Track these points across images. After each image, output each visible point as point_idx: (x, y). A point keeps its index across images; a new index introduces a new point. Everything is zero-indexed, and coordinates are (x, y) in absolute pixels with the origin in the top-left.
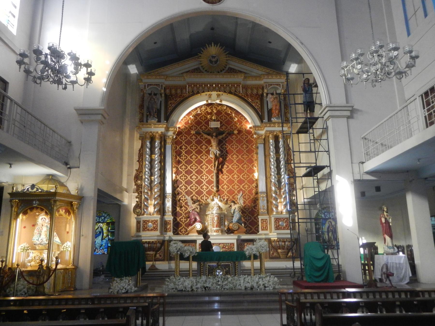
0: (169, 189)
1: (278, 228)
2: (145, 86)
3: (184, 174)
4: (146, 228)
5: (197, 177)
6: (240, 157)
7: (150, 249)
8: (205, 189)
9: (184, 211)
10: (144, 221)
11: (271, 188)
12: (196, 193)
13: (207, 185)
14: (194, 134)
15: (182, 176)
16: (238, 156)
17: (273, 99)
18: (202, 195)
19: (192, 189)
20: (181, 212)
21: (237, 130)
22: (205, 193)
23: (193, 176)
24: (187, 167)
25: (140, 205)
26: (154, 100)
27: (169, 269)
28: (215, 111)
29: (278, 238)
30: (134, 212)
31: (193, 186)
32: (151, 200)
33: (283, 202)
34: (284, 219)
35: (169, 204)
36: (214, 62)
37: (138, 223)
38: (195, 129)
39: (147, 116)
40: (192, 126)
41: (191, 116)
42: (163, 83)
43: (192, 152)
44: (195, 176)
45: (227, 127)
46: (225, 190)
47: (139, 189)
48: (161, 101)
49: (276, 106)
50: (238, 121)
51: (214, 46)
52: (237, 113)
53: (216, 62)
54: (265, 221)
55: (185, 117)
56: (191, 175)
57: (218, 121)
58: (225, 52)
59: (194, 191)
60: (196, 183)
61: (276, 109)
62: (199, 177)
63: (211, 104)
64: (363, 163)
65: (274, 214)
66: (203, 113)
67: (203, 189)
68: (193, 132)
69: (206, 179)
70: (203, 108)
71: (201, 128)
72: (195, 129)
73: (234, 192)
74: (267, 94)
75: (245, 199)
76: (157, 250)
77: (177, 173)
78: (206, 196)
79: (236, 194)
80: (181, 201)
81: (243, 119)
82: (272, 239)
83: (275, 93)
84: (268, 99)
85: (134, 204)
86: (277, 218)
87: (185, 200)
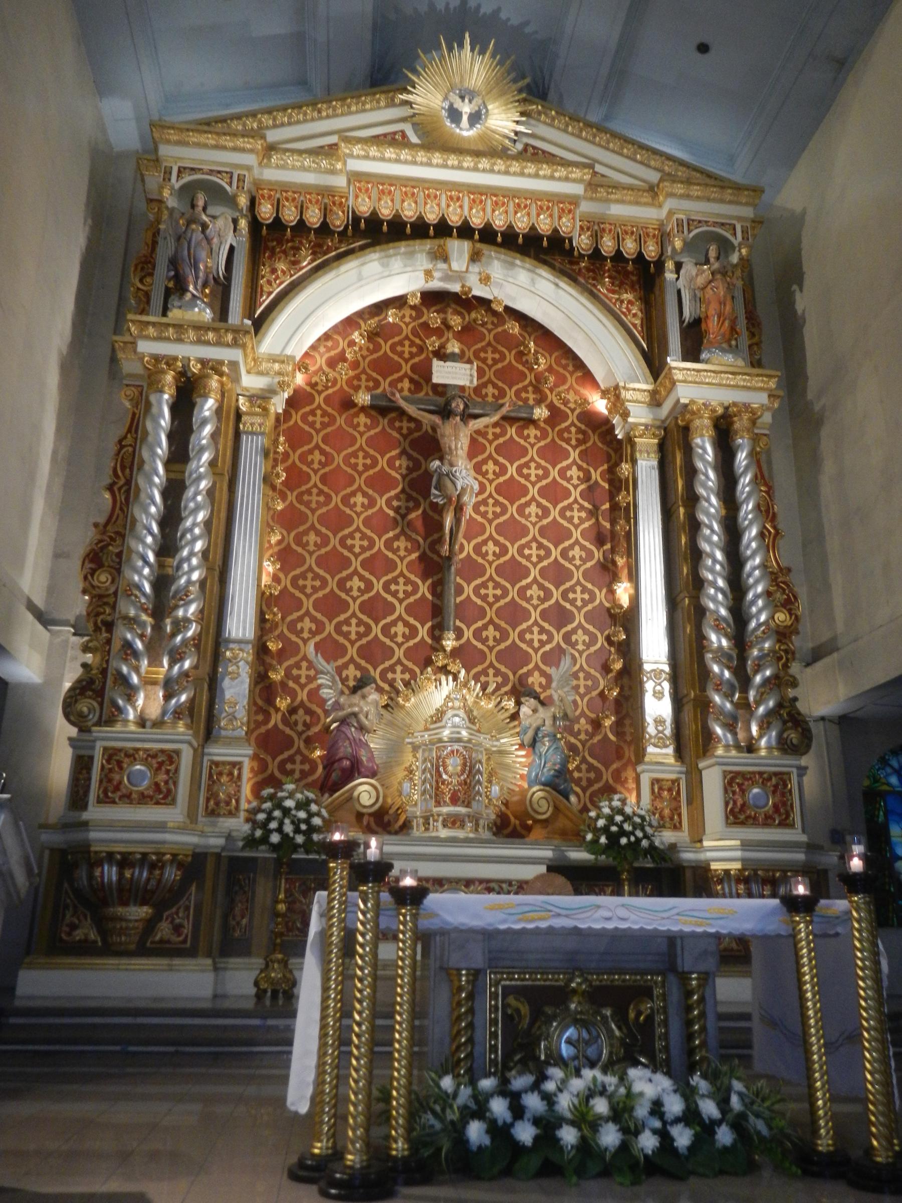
0: (241, 623)
1: (738, 815)
2: (168, 172)
3: (310, 569)
4: (117, 788)
5: (369, 586)
6: (555, 513)
7: (128, 893)
8: (400, 639)
9: (300, 728)
10: (111, 754)
12: (364, 652)
13: (412, 620)
14: (363, 409)
15: (303, 576)
16: (546, 512)
17: (707, 275)
18: (387, 664)
19: (346, 635)
20: (288, 731)
21: (548, 407)
22: (399, 653)
23: (350, 577)
24: (326, 541)
25: (97, 685)
26: (204, 226)
27: (215, 996)
29: (743, 860)
30: (67, 715)
31: (347, 622)
32: (155, 661)
33: (758, 703)
34: (764, 778)
35: (237, 689)
36: (465, 118)
37: (82, 764)
39: (168, 293)
41: (356, 336)
42: (249, 168)
43: (352, 480)
44: (362, 578)
46: (491, 649)
47: (101, 623)
48: (232, 249)
49: (722, 303)
50: (550, 369)
51: (472, 50)
53: (475, 118)
54: (670, 790)
55: (326, 336)
56: (344, 574)
57: (469, 362)
58: (515, 81)
59: (353, 643)
60: (363, 607)
62: (378, 586)
65: (720, 752)
66: (407, 331)
67: (392, 638)
69: (407, 594)
73: (527, 659)
74: (678, 266)
76: (164, 900)
77: (286, 557)
78: (405, 669)
79: (537, 667)
80: (291, 684)
81: (571, 368)
82: (714, 866)
84: (681, 284)
86: (738, 773)
87: (311, 679)
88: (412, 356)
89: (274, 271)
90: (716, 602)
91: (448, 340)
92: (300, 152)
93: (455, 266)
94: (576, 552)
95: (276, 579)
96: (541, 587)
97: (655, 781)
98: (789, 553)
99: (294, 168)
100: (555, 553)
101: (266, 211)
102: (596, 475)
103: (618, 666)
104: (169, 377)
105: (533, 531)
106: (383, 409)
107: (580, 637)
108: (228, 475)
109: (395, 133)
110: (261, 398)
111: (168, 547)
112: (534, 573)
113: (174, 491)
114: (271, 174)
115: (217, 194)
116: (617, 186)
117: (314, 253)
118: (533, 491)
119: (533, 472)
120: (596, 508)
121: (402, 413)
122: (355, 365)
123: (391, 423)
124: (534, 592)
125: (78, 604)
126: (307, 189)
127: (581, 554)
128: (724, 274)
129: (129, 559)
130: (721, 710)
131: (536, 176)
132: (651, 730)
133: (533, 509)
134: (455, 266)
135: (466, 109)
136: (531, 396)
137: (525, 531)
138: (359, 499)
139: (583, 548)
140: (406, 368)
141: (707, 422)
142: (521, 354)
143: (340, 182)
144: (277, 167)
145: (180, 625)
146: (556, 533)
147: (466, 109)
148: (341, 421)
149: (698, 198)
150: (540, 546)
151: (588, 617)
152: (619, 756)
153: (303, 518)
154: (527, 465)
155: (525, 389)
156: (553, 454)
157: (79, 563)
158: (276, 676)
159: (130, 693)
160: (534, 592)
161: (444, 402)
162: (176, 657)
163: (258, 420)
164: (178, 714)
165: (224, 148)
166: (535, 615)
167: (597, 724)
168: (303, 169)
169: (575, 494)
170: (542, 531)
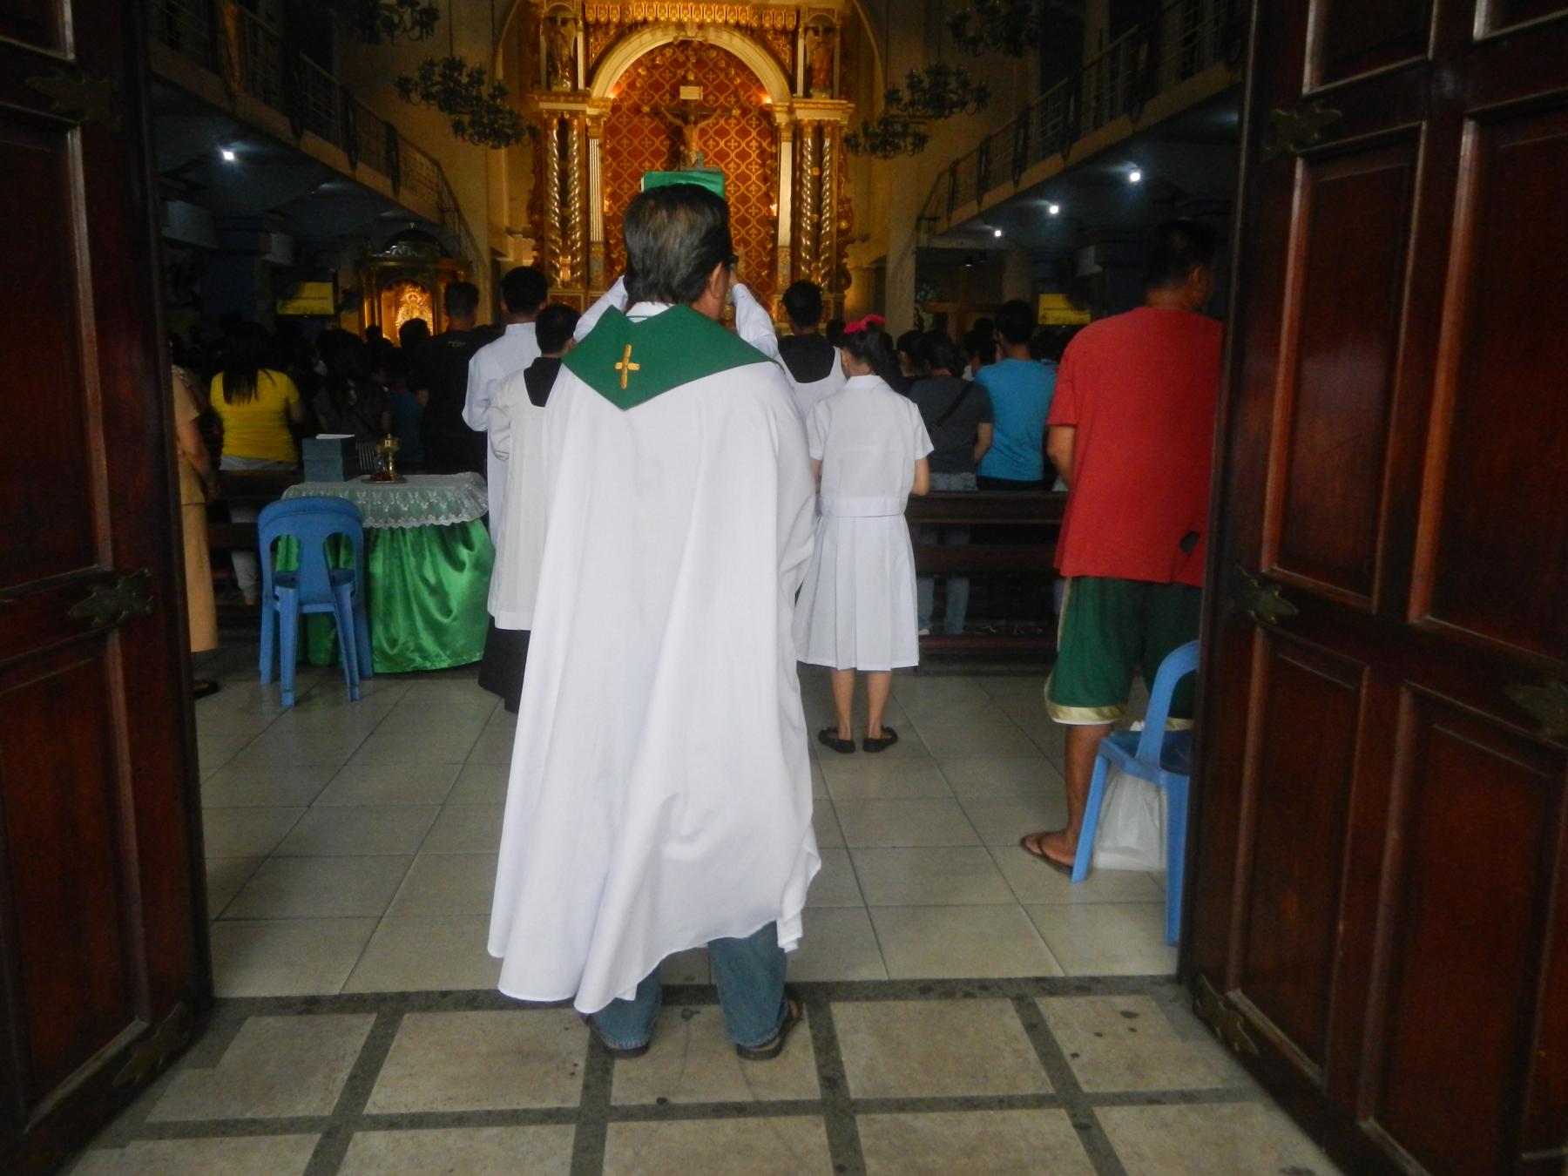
0: (597, 234)
6: (743, 167)
16: (739, 166)
28: (693, 60)
39: (549, 74)
50: (742, 84)
52: (742, 67)
57: (698, 83)
61: (820, 70)
64: (935, 219)
68: (646, 109)
70: (668, 52)
77: (613, 197)
83: (821, 29)
90: (807, 225)
94: (753, 188)
95: (610, 208)
98: (848, 191)
102: (765, 145)
106: (656, 112)
107: (753, 231)
108: (585, 165)
110: (595, 119)
111: (564, 203)
113: (564, 176)
115: (565, 9)
118: (733, 155)
125: (523, 223)
127: (755, 187)
133: (732, 165)
136: (733, 100)
138: (647, 164)
140: (667, 87)
145: (575, 242)
146: (743, 178)
148: (636, 120)
151: (758, 222)
153: (621, 176)
156: (743, 133)
157: (524, 208)
158: (614, 256)
159: (557, 272)
161: (684, 111)
162: (574, 257)
164: (577, 280)
167: (759, 274)
169: (754, 155)
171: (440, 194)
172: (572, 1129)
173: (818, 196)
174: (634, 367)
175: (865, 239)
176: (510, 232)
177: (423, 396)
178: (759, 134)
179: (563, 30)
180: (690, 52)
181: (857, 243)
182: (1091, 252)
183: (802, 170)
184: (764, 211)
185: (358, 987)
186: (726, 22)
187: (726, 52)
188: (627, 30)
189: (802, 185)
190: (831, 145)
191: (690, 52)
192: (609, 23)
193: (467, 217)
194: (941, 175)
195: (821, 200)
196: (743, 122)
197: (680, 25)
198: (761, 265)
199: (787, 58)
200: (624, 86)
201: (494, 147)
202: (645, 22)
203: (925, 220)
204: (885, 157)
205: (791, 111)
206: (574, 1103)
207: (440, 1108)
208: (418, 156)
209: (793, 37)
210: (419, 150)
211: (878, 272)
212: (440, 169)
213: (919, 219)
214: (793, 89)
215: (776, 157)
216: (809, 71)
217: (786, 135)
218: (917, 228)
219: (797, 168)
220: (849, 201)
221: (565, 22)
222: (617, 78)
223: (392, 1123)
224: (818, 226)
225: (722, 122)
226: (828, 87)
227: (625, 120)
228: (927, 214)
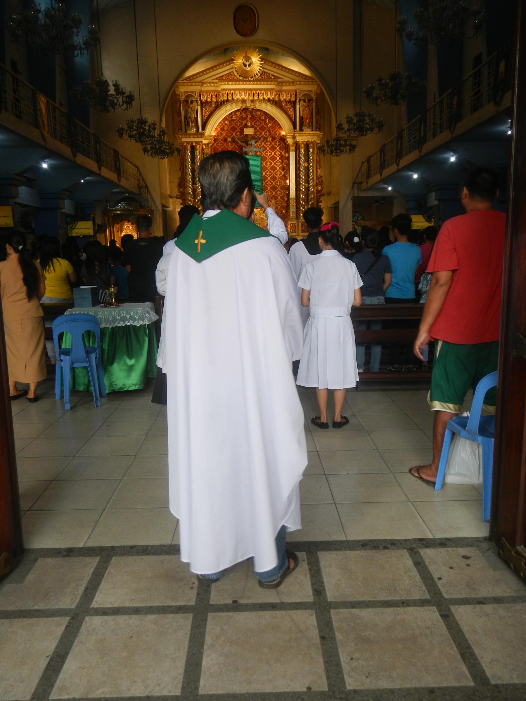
6: (273, 164)
11: (300, 196)
16: (271, 163)
26: (192, 108)
28: (250, 116)
38: (230, 136)
39: (185, 125)
40: (227, 133)
45: (261, 134)
47: (182, 196)
50: (272, 126)
52: (272, 118)
53: (250, 65)
55: (220, 123)
57: (252, 127)
61: (306, 118)
63: (245, 109)
64: (361, 183)
66: (238, 118)
68: (229, 139)
70: (238, 113)
71: (236, 134)
72: (230, 136)
75: (277, 204)
83: (306, 100)
85: (178, 210)
88: (240, 125)
89: (206, 109)
91: (248, 121)
92: (209, 83)
93: (248, 105)
96: (270, 182)
97: (291, 224)
99: (209, 87)
100: (273, 173)
101: (203, 100)
102: (283, 153)
103: (286, 199)
104: (189, 147)
105: (269, 168)
107: (279, 192)
109: (231, 73)
112: (269, 178)
114: (204, 89)
115: (192, 96)
116: (283, 82)
117: (215, 103)
118: (268, 159)
119: (269, 154)
120: (283, 161)
121: (238, 143)
122: (227, 130)
123: (236, 144)
124: (269, 183)
125: (176, 192)
126: (213, 91)
127: (279, 172)
128: (308, 106)
129: (187, 187)
130: (302, 210)
131: (264, 84)
132: (291, 214)
133: (268, 163)
134: (248, 105)
135: (247, 64)
136: (268, 133)
137: (267, 169)
139: (280, 172)
140: (238, 129)
141: (303, 145)
142: (265, 122)
143: (219, 89)
144: (205, 87)
147: (247, 64)
149: (303, 84)
150: (270, 172)
152: (287, 218)
154: (267, 152)
155: (266, 132)
156: (273, 148)
160: (269, 183)
163: (207, 150)
165: (192, 85)
166: (269, 188)
167: (282, 211)
168: (211, 86)
169: (278, 158)
170: (271, 168)
171: (139, 182)
172: (191, 616)
173: (307, 176)
174: (203, 241)
175: (329, 194)
176: (171, 197)
177: (129, 268)
178: (280, 148)
179: (191, 106)
180: (248, 113)
181: (325, 196)
182: (433, 194)
183: (300, 164)
184: (283, 183)
185: (92, 543)
186: (264, 99)
187: (264, 112)
188: (219, 104)
189: (300, 171)
190: (313, 152)
191: (248, 113)
192: (212, 101)
193: (151, 190)
194: (363, 163)
195: (309, 177)
196: (273, 143)
197: (244, 101)
198: (283, 207)
199: (292, 114)
200: (219, 129)
201: (161, 158)
202: (228, 100)
203: (356, 184)
204: (337, 156)
205: (294, 137)
206: (192, 603)
207: (127, 604)
208: (129, 164)
209: (294, 104)
210: (129, 161)
211: (335, 208)
212: (139, 170)
213: (354, 183)
214: (295, 127)
215: (288, 159)
216: (301, 119)
217: (292, 148)
218: (353, 187)
219: (297, 163)
220: (321, 177)
221: (192, 102)
222: (216, 126)
223: (104, 612)
224: (308, 189)
225: (263, 143)
226: (310, 126)
227: (220, 145)
228: (357, 181)
